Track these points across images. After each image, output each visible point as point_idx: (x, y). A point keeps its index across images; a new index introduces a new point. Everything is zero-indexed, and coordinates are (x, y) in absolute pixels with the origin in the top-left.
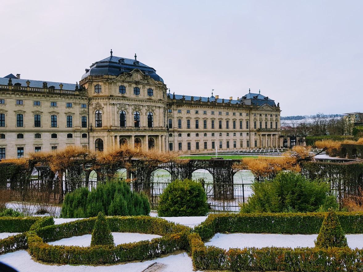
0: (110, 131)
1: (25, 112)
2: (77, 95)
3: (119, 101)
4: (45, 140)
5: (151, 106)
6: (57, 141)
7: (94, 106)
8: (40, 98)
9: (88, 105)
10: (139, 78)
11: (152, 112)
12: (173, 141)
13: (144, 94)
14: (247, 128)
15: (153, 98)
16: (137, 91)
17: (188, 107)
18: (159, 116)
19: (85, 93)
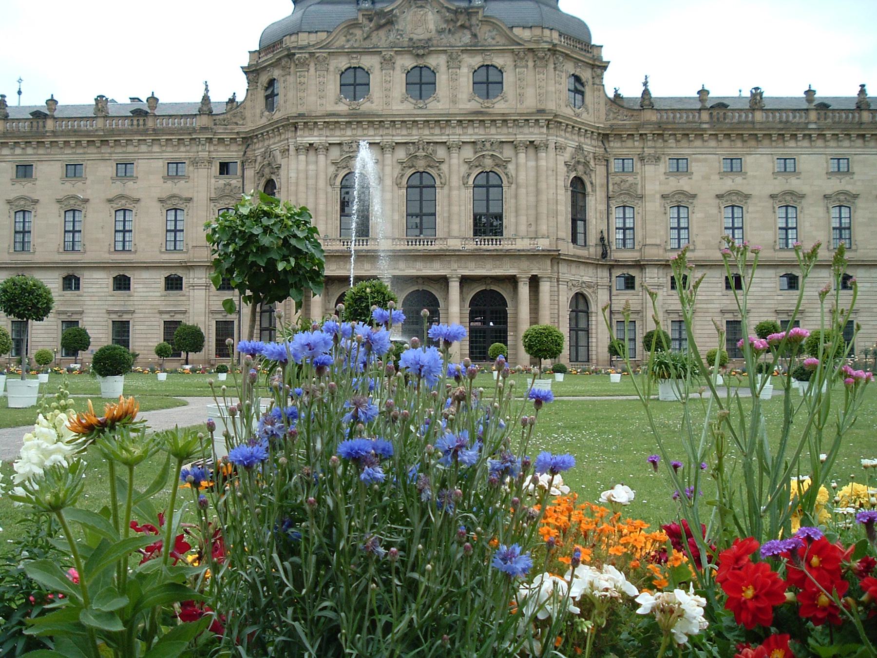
1: (36, 202)
3: (338, 133)
4: (94, 298)
5: (488, 145)
6: (131, 303)
7: (258, 167)
8: (81, 151)
10: (432, 26)
11: (497, 169)
12: (637, 312)
13: (454, 90)
16: (421, 83)
17: (726, 143)
18: (532, 189)
19: (234, 120)
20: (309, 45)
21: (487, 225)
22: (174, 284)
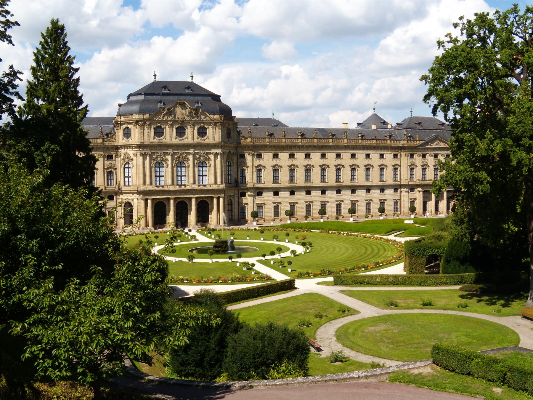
0: (139, 193)
7: (122, 157)
9: (116, 156)
11: (206, 162)
14: (395, 178)
16: (181, 132)
20: (144, 119)
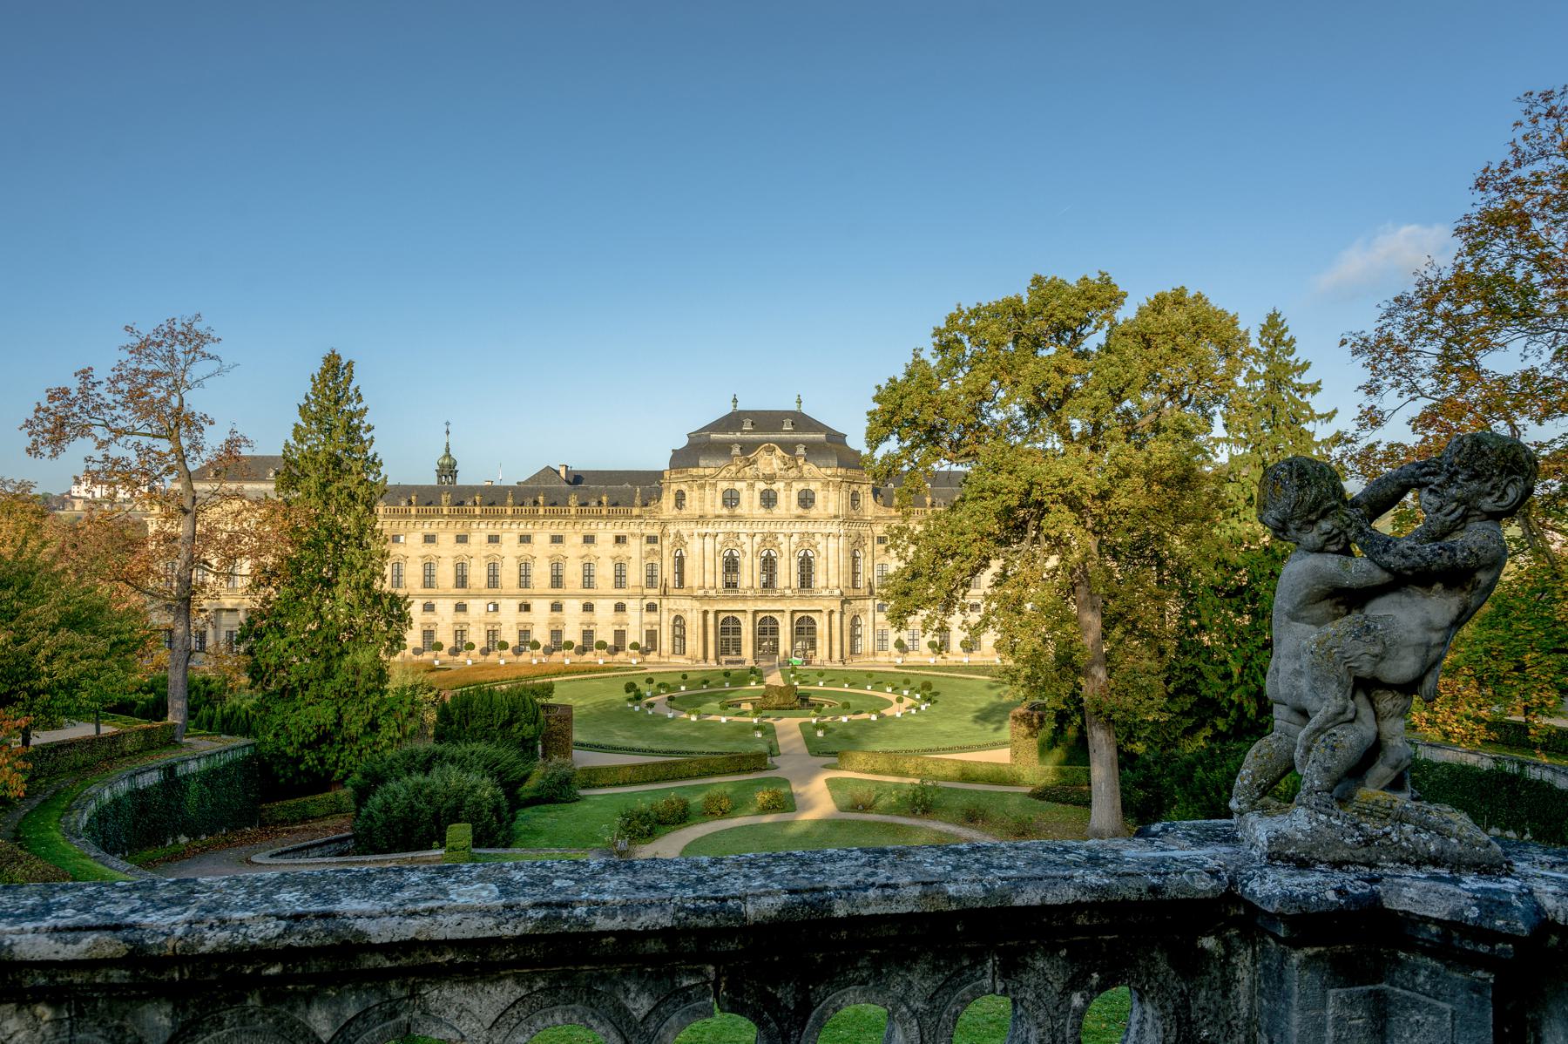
2: (639, 517)
13: (787, 501)
15: (813, 512)
16: (769, 500)
21: (806, 580)
22: (620, 608)
